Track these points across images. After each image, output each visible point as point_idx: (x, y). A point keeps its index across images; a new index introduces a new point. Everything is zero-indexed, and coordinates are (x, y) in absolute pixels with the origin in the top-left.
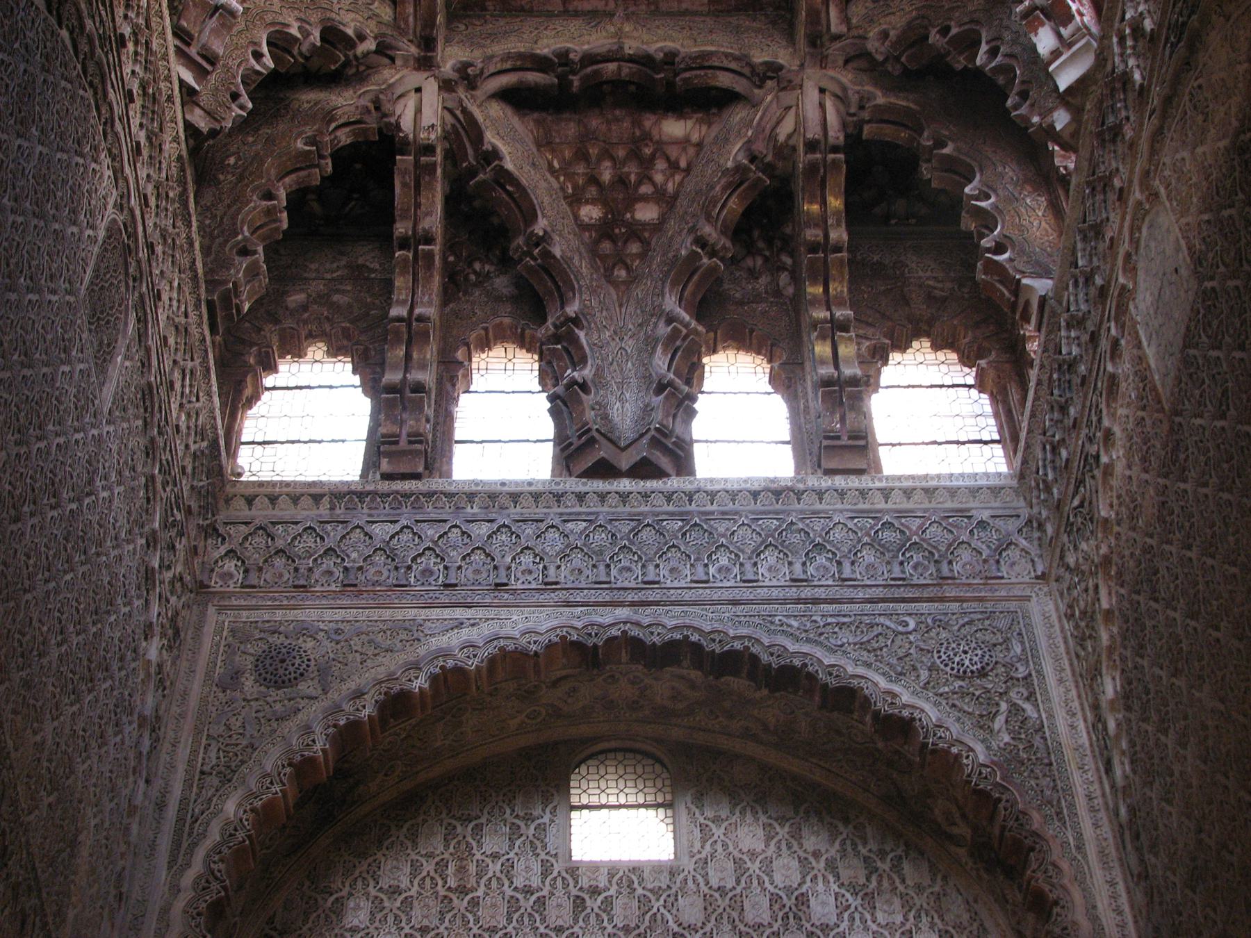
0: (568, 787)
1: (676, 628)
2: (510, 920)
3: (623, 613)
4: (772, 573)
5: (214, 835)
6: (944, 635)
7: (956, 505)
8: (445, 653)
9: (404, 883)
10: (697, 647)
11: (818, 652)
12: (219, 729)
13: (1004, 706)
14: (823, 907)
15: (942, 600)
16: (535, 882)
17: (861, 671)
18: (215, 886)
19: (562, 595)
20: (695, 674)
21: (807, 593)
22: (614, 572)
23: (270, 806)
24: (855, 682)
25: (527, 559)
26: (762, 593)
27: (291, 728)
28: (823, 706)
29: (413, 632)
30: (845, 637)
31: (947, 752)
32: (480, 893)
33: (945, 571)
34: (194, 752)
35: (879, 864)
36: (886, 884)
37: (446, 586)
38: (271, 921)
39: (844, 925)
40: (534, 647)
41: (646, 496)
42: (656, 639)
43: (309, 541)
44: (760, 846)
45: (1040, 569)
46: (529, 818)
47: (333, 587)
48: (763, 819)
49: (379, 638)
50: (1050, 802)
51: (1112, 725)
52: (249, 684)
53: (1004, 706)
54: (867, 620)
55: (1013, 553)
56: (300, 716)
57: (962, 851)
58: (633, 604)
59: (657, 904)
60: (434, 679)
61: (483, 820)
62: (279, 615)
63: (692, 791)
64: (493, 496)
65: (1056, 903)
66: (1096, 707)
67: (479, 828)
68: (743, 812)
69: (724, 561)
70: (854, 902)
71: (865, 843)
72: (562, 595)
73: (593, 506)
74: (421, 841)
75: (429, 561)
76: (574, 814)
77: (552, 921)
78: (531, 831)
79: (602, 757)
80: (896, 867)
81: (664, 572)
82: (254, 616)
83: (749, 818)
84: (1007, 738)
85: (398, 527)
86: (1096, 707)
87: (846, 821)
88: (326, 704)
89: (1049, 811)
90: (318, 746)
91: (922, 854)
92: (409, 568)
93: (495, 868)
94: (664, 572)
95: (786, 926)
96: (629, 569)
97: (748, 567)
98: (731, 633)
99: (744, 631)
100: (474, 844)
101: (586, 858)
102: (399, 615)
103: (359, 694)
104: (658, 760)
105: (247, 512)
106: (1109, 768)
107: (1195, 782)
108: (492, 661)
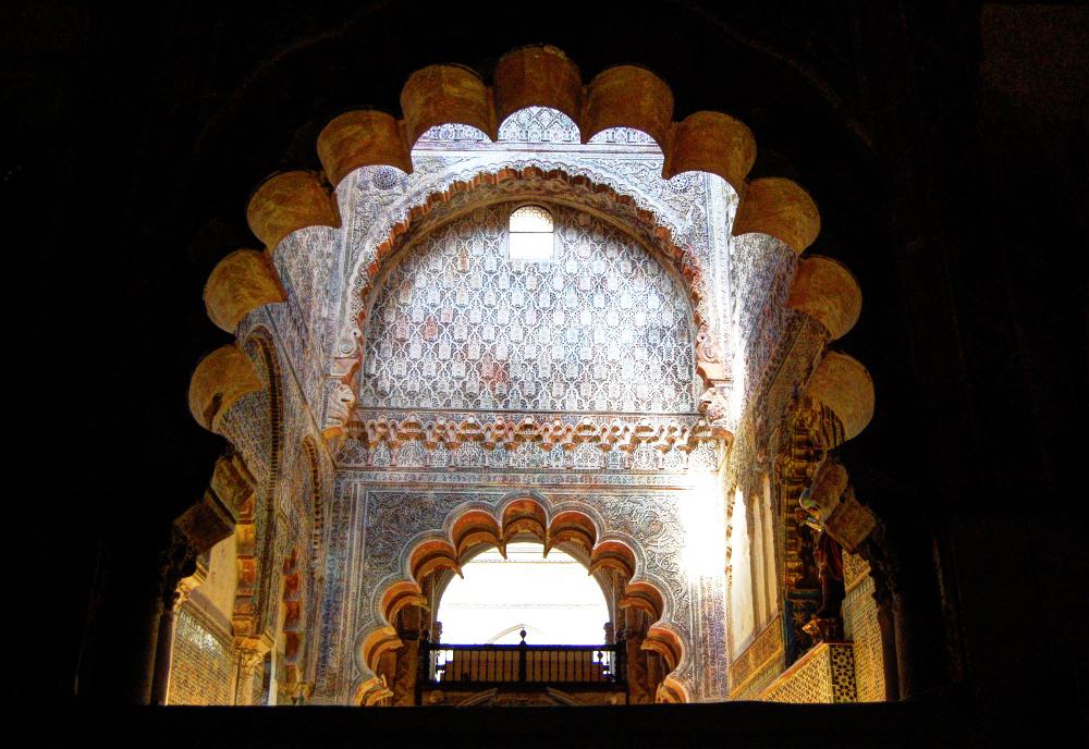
0: (506, 223)
3: (533, 155)
5: (361, 260)
8: (454, 174)
9: (440, 268)
10: (564, 173)
11: (616, 178)
12: (359, 209)
13: (692, 208)
14: (612, 284)
16: (494, 269)
17: (634, 188)
18: (363, 282)
19: (507, 146)
21: (613, 148)
23: (384, 245)
24: (630, 194)
27: (390, 208)
30: (628, 170)
31: (665, 228)
34: (351, 220)
36: (639, 273)
39: (620, 292)
40: (493, 172)
46: (491, 239)
48: (591, 242)
49: (427, 165)
52: (371, 185)
53: (692, 208)
57: (672, 263)
59: (544, 280)
60: (451, 186)
66: (727, 215)
67: (471, 243)
68: (582, 238)
70: (626, 281)
78: (492, 246)
80: (644, 266)
81: (551, 135)
84: (691, 223)
86: (727, 215)
87: (626, 244)
89: (702, 257)
90: (403, 218)
93: (477, 262)
95: (597, 291)
99: (584, 166)
104: (548, 211)
108: (476, 178)
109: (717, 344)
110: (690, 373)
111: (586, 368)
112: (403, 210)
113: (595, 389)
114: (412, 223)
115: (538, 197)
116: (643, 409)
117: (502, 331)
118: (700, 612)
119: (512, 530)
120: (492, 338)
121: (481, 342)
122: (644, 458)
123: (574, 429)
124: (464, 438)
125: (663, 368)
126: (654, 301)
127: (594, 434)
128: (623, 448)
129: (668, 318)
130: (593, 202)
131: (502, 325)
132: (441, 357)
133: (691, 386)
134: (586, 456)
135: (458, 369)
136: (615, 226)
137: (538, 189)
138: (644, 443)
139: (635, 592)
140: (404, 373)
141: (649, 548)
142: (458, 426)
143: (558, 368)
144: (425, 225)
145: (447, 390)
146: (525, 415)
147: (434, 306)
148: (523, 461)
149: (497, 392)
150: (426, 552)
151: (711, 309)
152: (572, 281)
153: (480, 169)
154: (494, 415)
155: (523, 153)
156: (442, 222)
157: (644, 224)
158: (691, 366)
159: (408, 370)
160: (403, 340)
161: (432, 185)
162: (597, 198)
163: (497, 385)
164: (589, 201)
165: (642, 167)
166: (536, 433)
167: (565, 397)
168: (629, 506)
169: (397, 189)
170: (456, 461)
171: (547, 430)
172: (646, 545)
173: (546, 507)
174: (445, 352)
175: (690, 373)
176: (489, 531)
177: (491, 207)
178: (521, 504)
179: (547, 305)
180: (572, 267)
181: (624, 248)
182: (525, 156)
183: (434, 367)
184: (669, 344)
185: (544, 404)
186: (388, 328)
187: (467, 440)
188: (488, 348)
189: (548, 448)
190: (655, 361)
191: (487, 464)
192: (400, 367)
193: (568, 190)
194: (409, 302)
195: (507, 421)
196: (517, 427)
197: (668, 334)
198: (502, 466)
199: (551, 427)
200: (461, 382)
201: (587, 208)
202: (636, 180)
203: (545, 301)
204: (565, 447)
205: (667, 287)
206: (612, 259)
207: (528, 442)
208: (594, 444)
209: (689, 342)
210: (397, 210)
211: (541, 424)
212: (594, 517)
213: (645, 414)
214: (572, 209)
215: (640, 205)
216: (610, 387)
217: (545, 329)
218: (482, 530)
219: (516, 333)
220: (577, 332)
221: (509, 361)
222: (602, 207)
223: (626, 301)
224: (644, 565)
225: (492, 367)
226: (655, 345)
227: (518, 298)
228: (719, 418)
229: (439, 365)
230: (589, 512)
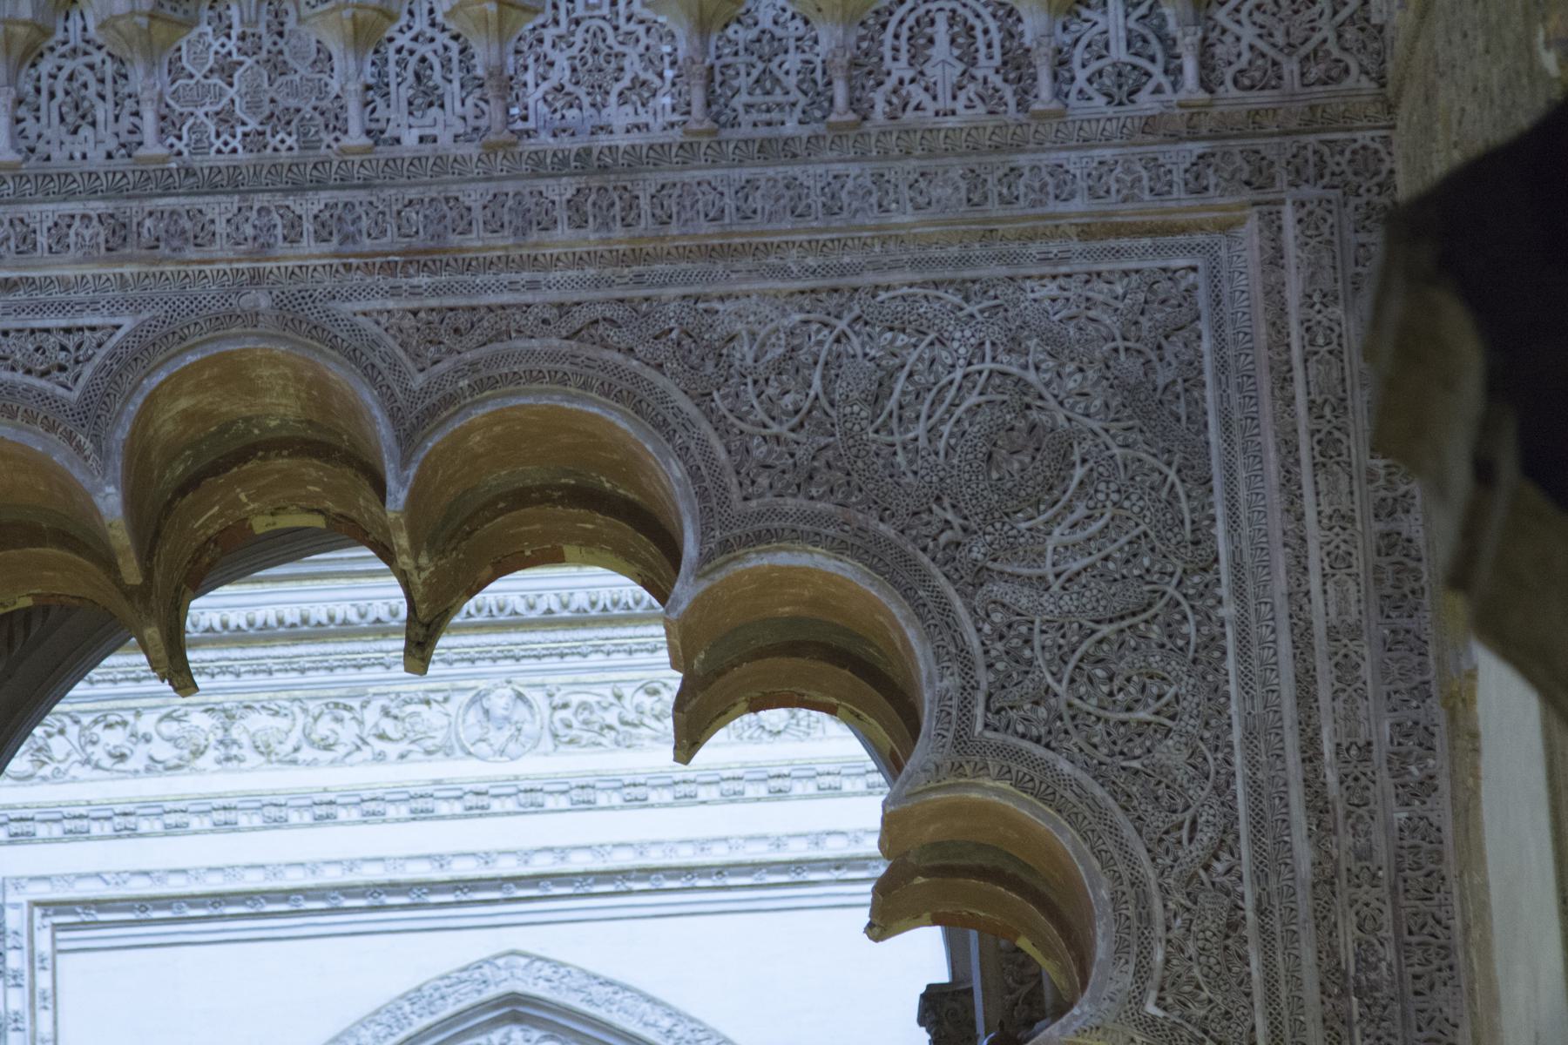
118: (1308, 955)
119: (207, 519)
122: (942, 62)
141: (997, 589)
148: (225, 118)
172: (980, 575)
176: (64, 539)
218: (34, 536)
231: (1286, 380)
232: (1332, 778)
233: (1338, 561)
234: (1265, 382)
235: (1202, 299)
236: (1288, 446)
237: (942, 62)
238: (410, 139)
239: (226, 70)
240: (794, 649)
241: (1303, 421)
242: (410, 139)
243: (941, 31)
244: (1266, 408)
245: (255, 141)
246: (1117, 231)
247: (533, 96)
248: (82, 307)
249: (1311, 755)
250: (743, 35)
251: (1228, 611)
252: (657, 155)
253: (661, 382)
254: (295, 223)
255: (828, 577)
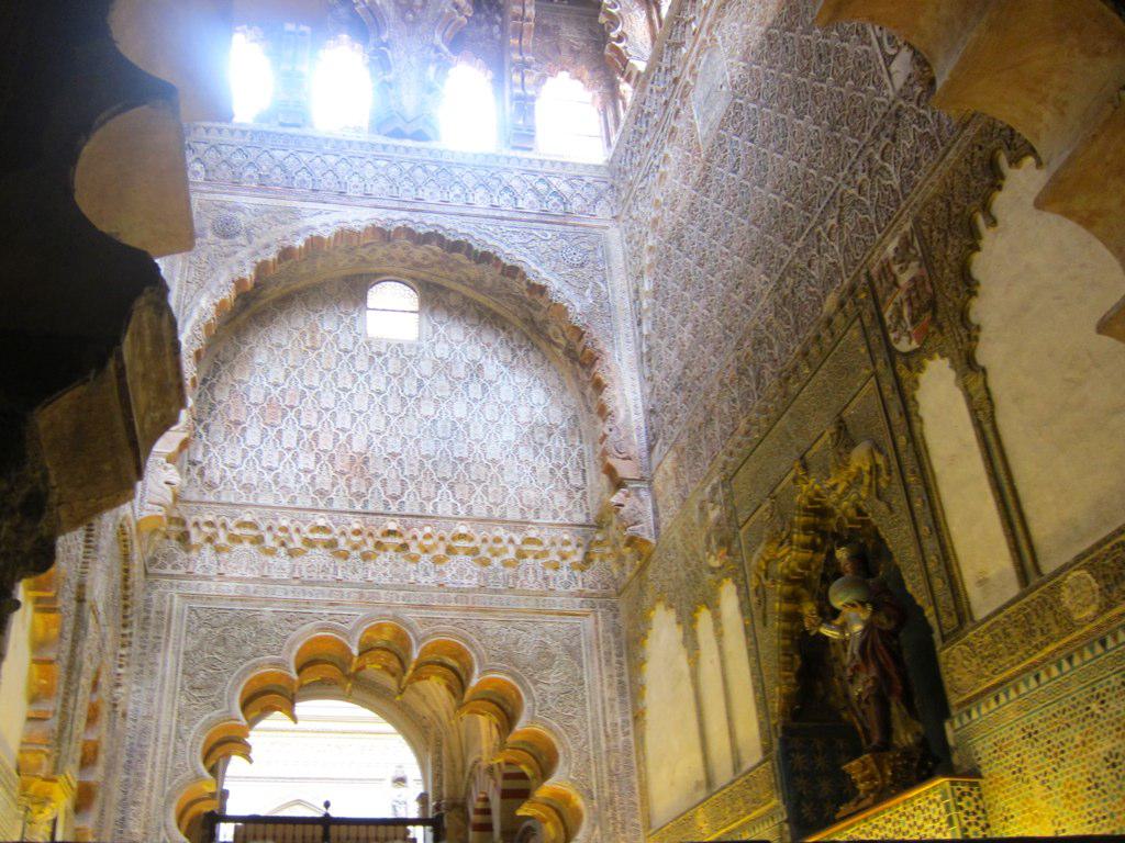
1: (432, 225)
2: (337, 365)
3: (404, 214)
4: (480, 201)
6: (565, 243)
7: (576, 173)
8: (313, 229)
9: (284, 342)
10: (441, 238)
15: (565, 224)
16: (350, 347)
17: (522, 258)
19: (374, 202)
20: (437, 249)
21: (498, 214)
22: (401, 191)
24: (519, 264)
25: (355, 179)
26: (475, 212)
28: (502, 273)
29: (295, 214)
30: (516, 238)
31: (561, 305)
32: (322, 350)
33: (569, 210)
35: (518, 352)
37: (313, 190)
38: (217, 356)
40: (358, 229)
41: (418, 150)
42: (421, 231)
43: (238, 158)
44: (462, 338)
45: (615, 214)
46: (347, 314)
47: (254, 185)
48: (464, 324)
50: (608, 336)
51: (645, 305)
53: (591, 284)
54: (528, 231)
55: (602, 203)
56: (237, 255)
58: (409, 210)
59: (410, 364)
60: (307, 242)
61: (324, 312)
62: (225, 197)
63: (429, 307)
64: (338, 142)
65: (606, 386)
66: (637, 291)
68: (454, 319)
69: (458, 192)
70: (505, 370)
71: (512, 339)
72: (374, 202)
73: (390, 152)
74: (292, 321)
75: (304, 175)
76: (368, 312)
77: (358, 368)
79: (383, 284)
80: (526, 355)
82: (212, 197)
83: (457, 323)
85: (287, 154)
86: (637, 291)
87: (504, 329)
88: (250, 250)
91: (539, 349)
92: (293, 178)
93: (330, 338)
94: (427, 194)
96: (408, 190)
97: (471, 198)
98: (460, 231)
100: (320, 325)
101: (375, 336)
102: (288, 204)
103: (267, 246)
104: (412, 288)
105: (205, 137)
106: (640, 323)
107: (687, 344)
108: (336, 234)
109: (628, 437)
110: (584, 479)
111: (461, 467)
112: (247, 263)
113: (472, 492)
114: (256, 285)
115: (402, 271)
116: (530, 516)
117: (360, 419)
118: (604, 766)
120: (348, 426)
121: (334, 430)
122: (531, 576)
123: (448, 537)
124: (310, 543)
125: (552, 471)
126: (538, 395)
127: (472, 545)
128: (506, 564)
129: (556, 415)
130: (469, 279)
131: (360, 412)
132: (286, 445)
133: (585, 493)
134: (461, 571)
135: (307, 461)
136: (490, 309)
137: (403, 260)
138: (530, 560)
139: (518, 742)
140: (238, 462)
142: (305, 529)
143: (428, 465)
144: (269, 292)
145: (291, 484)
146: (389, 518)
147: (276, 385)
148: (385, 574)
149: (354, 490)
150: (257, 686)
151: (619, 398)
152: (443, 367)
153: (342, 225)
154: (350, 517)
155: (394, 212)
156: (287, 290)
157: (530, 305)
158: (584, 470)
159: (243, 458)
160: (237, 423)
161: (284, 239)
162: (474, 271)
163: (354, 481)
164: (464, 278)
165: (533, 237)
166: (399, 541)
167: (437, 500)
168: (514, 634)
169: (241, 239)
170: (300, 572)
171: (415, 537)
173: (411, 630)
174: (290, 438)
175: (584, 479)
176: (332, 663)
177: (346, 279)
178: (379, 628)
179: (414, 392)
180: (442, 350)
181: (503, 335)
182: (396, 215)
183: (276, 456)
184: (557, 444)
185: (411, 507)
186: (220, 407)
187: (314, 546)
188: (343, 437)
189: (415, 559)
190: (543, 464)
191: (340, 576)
192: (232, 455)
193: (439, 263)
194: (246, 379)
195: (366, 525)
196: (378, 533)
197: (557, 432)
198: (358, 581)
199: (420, 535)
200: (309, 476)
201: (463, 289)
202: (524, 250)
203: (410, 387)
204: (438, 560)
205: (553, 381)
206: (489, 345)
207: (391, 552)
208: (470, 558)
209: (581, 442)
210: (241, 263)
211: (408, 529)
212: (471, 646)
213: (533, 524)
214: (441, 287)
215: (532, 279)
216: (490, 490)
217: (411, 418)
219: (377, 422)
220: (449, 425)
221: (368, 455)
222: (477, 285)
223: (506, 393)
224: (534, 705)
225: (347, 460)
226: (541, 444)
227: (378, 382)
228: (636, 523)
229: (282, 456)
230: (466, 641)
231: (598, 647)
232: (609, 730)
233: (610, 685)
234: (594, 645)
235: (581, 630)
236: (600, 661)
237: (531, 576)
238: (423, 582)
239: (385, 564)
240: (483, 699)
241: (602, 655)
242: (423, 582)
243: (531, 571)
244: (595, 652)
245: (391, 579)
246: (565, 614)
247: (449, 575)
248: (352, 610)
249: (605, 725)
250: (490, 567)
251: (587, 694)
252: (473, 590)
253: (472, 636)
254: (398, 597)
255: (506, 682)
